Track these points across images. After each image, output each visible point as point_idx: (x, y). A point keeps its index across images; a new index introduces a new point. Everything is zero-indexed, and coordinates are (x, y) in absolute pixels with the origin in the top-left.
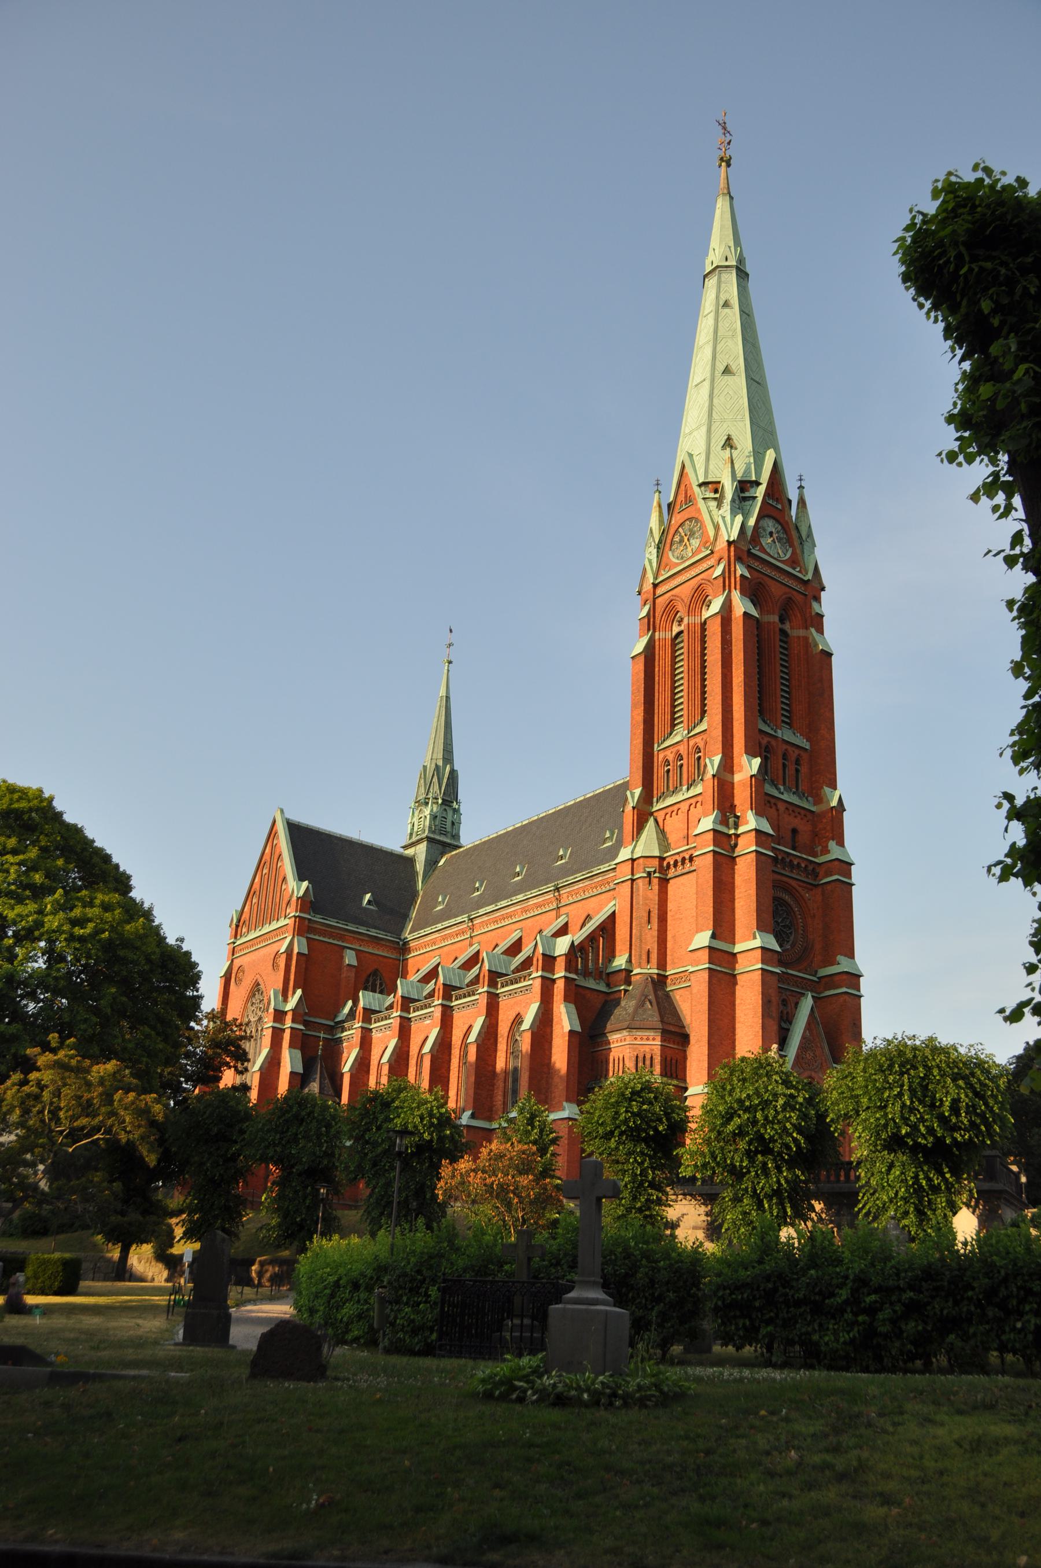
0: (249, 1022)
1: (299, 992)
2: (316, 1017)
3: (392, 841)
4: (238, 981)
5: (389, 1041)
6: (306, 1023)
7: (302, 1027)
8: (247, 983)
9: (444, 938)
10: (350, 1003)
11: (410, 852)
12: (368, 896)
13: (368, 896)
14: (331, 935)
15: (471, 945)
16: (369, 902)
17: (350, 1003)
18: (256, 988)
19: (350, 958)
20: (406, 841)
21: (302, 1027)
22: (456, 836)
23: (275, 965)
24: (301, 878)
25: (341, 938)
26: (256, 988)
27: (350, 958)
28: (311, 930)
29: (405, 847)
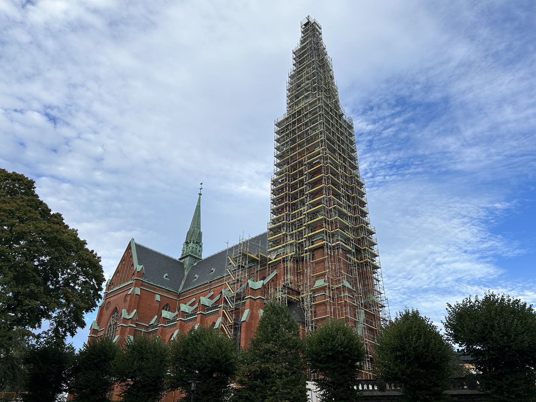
0: (111, 325)
1: (135, 311)
2: (141, 322)
3: (176, 255)
4: (107, 308)
5: (174, 331)
6: (137, 324)
7: (135, 326)
8: (112, 308)
9: (197, 290)
10: (156, 317)
11: (182, 261)
12: (166, 274)
13: (166, 274)
14: (150, 288)
15: (210, 292)
16: (166, 277)
17: (156, 317)
18: (116, 310)
19: (158, 298)
20: (180, 257)
21: (135, 326)
22: (201, 256)
23: (125, 300)
24: (140, 264)
25: (154, 289)
26: (116, 310)
27: (158, 298)
28: (142, 285)
29: (180, 259)
